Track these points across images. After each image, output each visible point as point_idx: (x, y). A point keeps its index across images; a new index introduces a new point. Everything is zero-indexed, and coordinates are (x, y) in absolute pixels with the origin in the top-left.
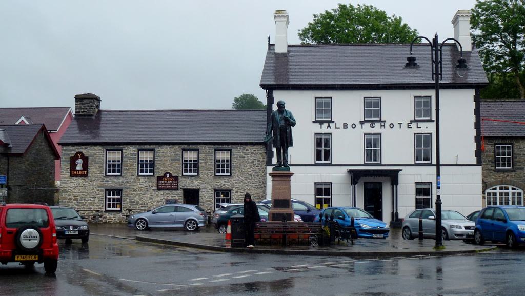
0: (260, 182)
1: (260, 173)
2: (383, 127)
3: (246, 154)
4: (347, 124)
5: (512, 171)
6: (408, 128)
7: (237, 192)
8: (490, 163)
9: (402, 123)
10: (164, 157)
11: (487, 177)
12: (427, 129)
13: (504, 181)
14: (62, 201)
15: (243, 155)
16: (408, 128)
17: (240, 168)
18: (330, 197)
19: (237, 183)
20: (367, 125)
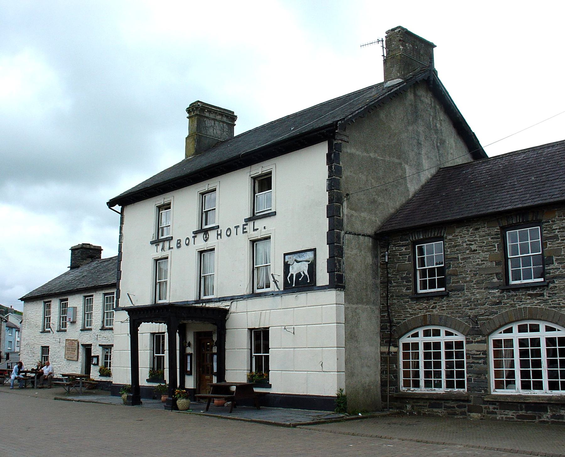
11: (399, 312)
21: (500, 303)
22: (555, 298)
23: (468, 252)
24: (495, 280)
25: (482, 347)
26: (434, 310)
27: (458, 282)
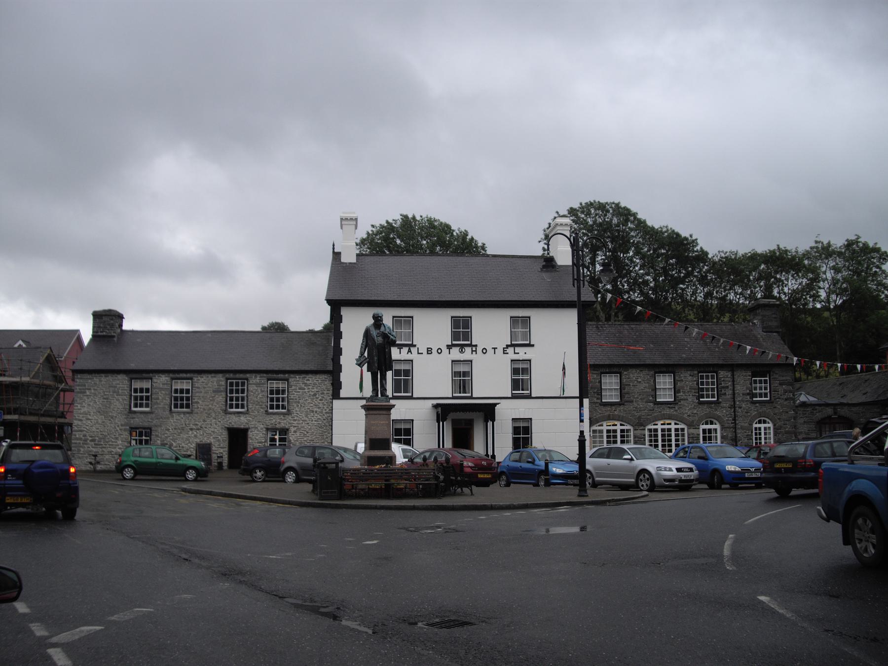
0: (324, 420)
1: (324, 408)
2: (474, 353)
3: (306, 385)
4: (432, 349)
5: (620, 405)
6: (504, 353)
7: (295, 432)
8: (596, 395)
9: (497, 348)
10: (205, 388)
12: (525, 355)
13: (611, 416)
14: (76, 443)
15: (303, 386)
16: (504, 353)
17: (299, 402)
18: (411, 437)
19: (295, 420)
20: (455, 350)
21: (653, 410)
22: (681, 409)
23: (636, 382)
24: (651, 398)
25: (642, 432)
26: (615, 412)
27: (630, 398)
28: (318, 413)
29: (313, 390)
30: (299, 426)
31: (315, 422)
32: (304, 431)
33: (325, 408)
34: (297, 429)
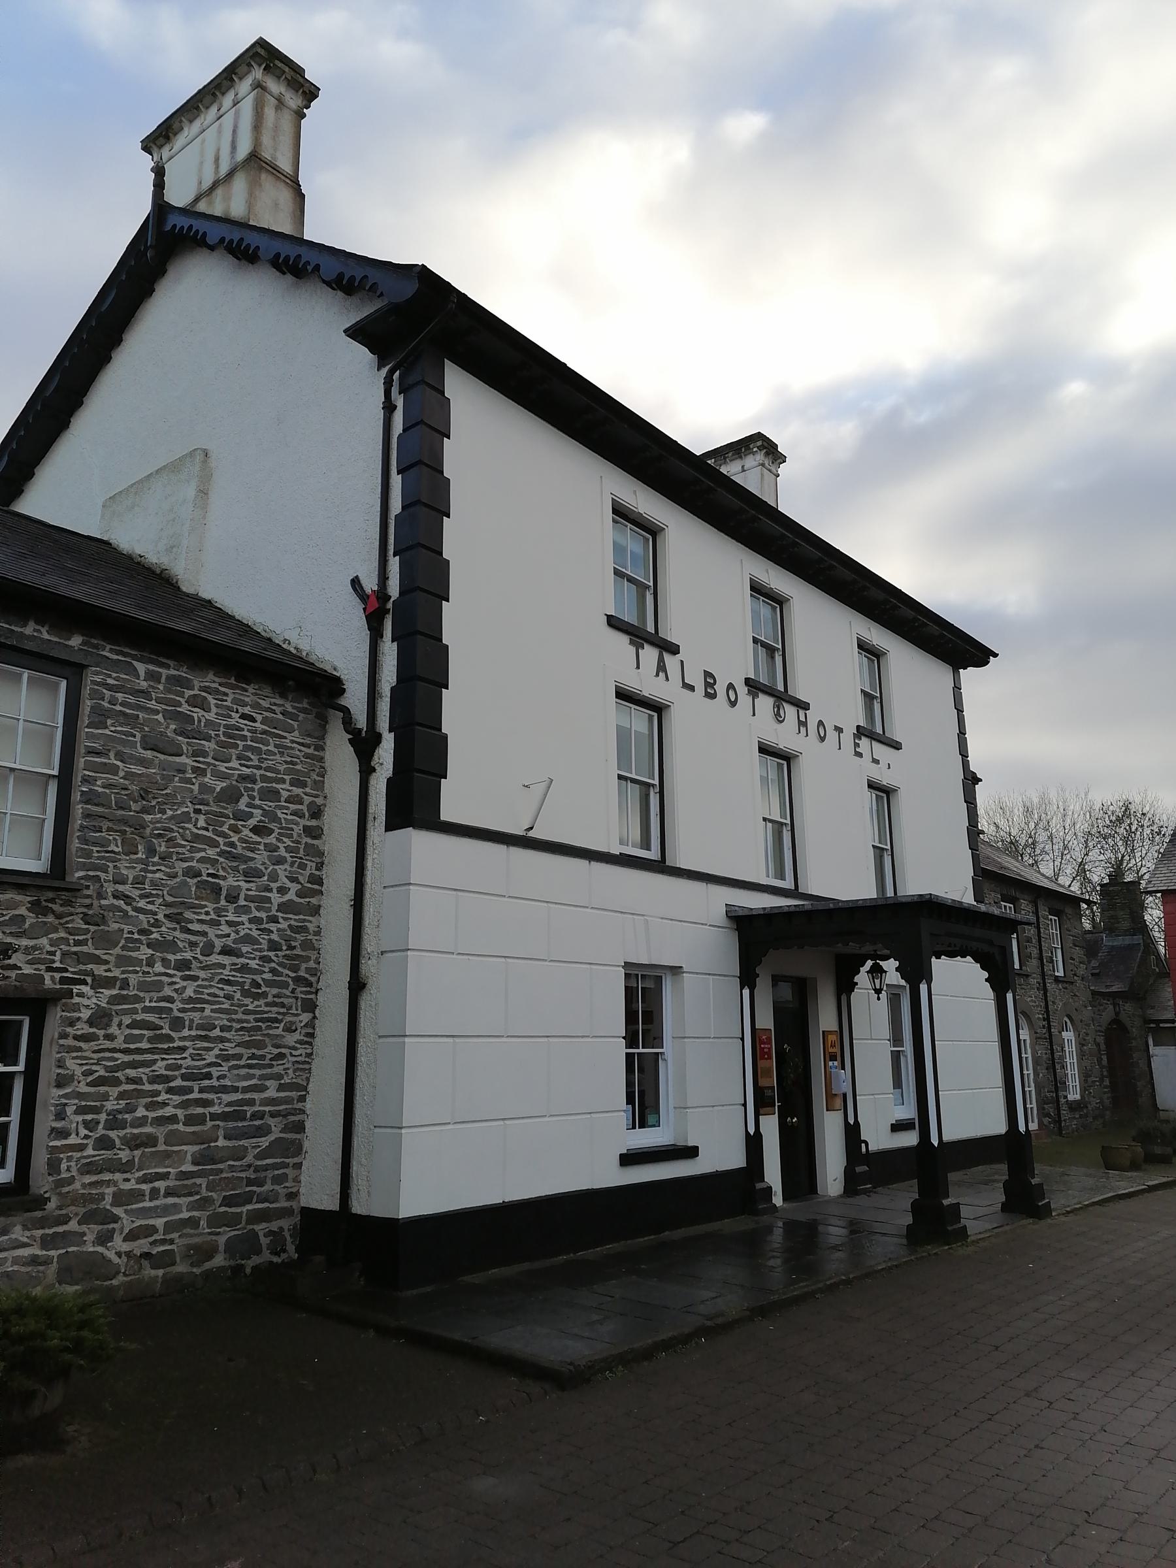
0: (274, 946)
1: (274, 877)
7: (100, 1018)
19: (107, 940)
28: (242, 902)
29: (222, 767)
30: (133, 979)
31: (226, 960)
32: (160, 1010)
33: (283, 880)
34: (113, 1000)
